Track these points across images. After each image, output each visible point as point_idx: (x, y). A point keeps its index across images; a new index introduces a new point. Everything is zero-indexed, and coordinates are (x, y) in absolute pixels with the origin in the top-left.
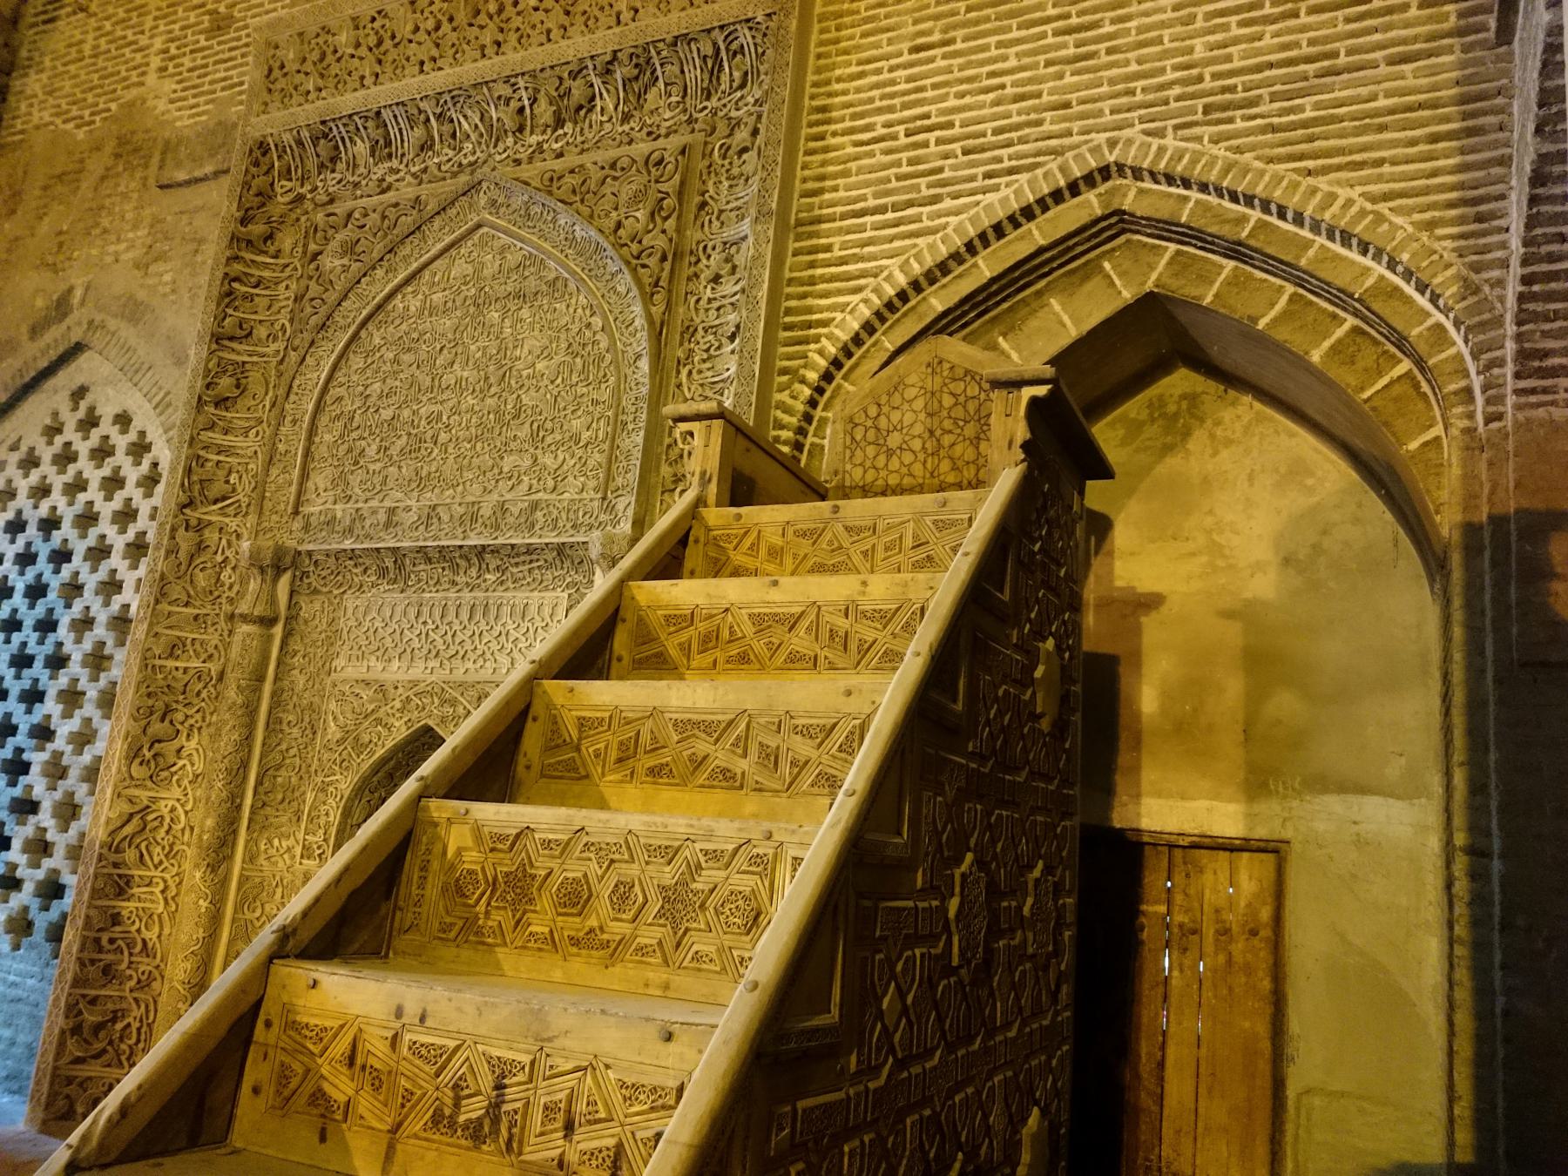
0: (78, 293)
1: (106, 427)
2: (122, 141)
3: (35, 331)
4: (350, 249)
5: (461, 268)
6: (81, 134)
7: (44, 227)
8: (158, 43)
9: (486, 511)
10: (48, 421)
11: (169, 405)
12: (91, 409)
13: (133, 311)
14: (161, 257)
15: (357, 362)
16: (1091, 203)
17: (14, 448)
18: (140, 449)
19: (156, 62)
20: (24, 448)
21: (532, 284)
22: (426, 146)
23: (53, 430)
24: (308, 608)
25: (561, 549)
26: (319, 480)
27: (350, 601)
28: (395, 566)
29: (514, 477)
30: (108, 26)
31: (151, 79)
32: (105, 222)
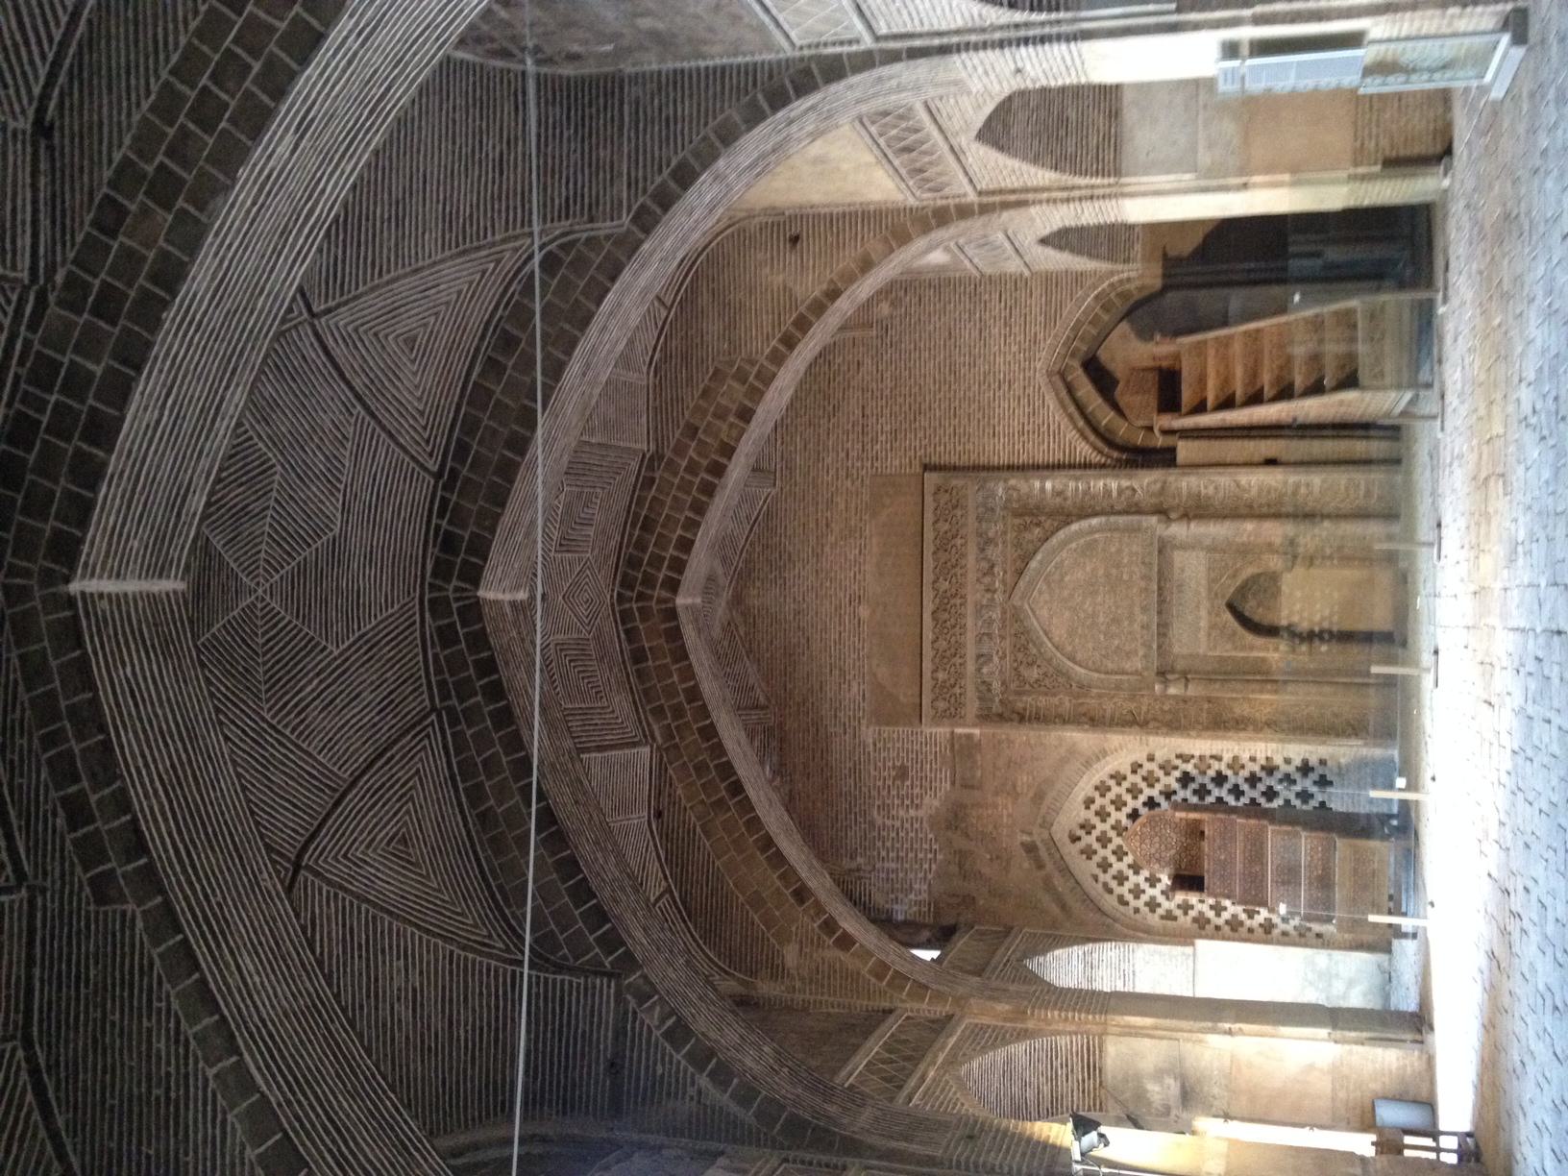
0: (1026, 838)
1: (1090, 815)
2: (948, 828)
3: (1041, 866)
4: (1030, 665)
5: (1045, 613)
6: (940, 857)
7: (986, 870)
8: (902, 813)
9: (1143, 584)
12: (1082, 827)
13: (1039, 797)
14: (1014, 787)
15: (1079, 656)
16: (1056, 378)
17: (1096, 878)
18: (1102, 789)
19: (912, 812)
20: (1098, 871)
21: (1056, 577)
22: (989, 635)
23: (1089, 853)
24: (1179, 667)
25: (1160, 552)
26: (1128, 666)
27: (1176, 650)
28: (1163, 628)
29: (1131, 573)
30: (883, 853)
31: (921, 813)
32: (991, 827)
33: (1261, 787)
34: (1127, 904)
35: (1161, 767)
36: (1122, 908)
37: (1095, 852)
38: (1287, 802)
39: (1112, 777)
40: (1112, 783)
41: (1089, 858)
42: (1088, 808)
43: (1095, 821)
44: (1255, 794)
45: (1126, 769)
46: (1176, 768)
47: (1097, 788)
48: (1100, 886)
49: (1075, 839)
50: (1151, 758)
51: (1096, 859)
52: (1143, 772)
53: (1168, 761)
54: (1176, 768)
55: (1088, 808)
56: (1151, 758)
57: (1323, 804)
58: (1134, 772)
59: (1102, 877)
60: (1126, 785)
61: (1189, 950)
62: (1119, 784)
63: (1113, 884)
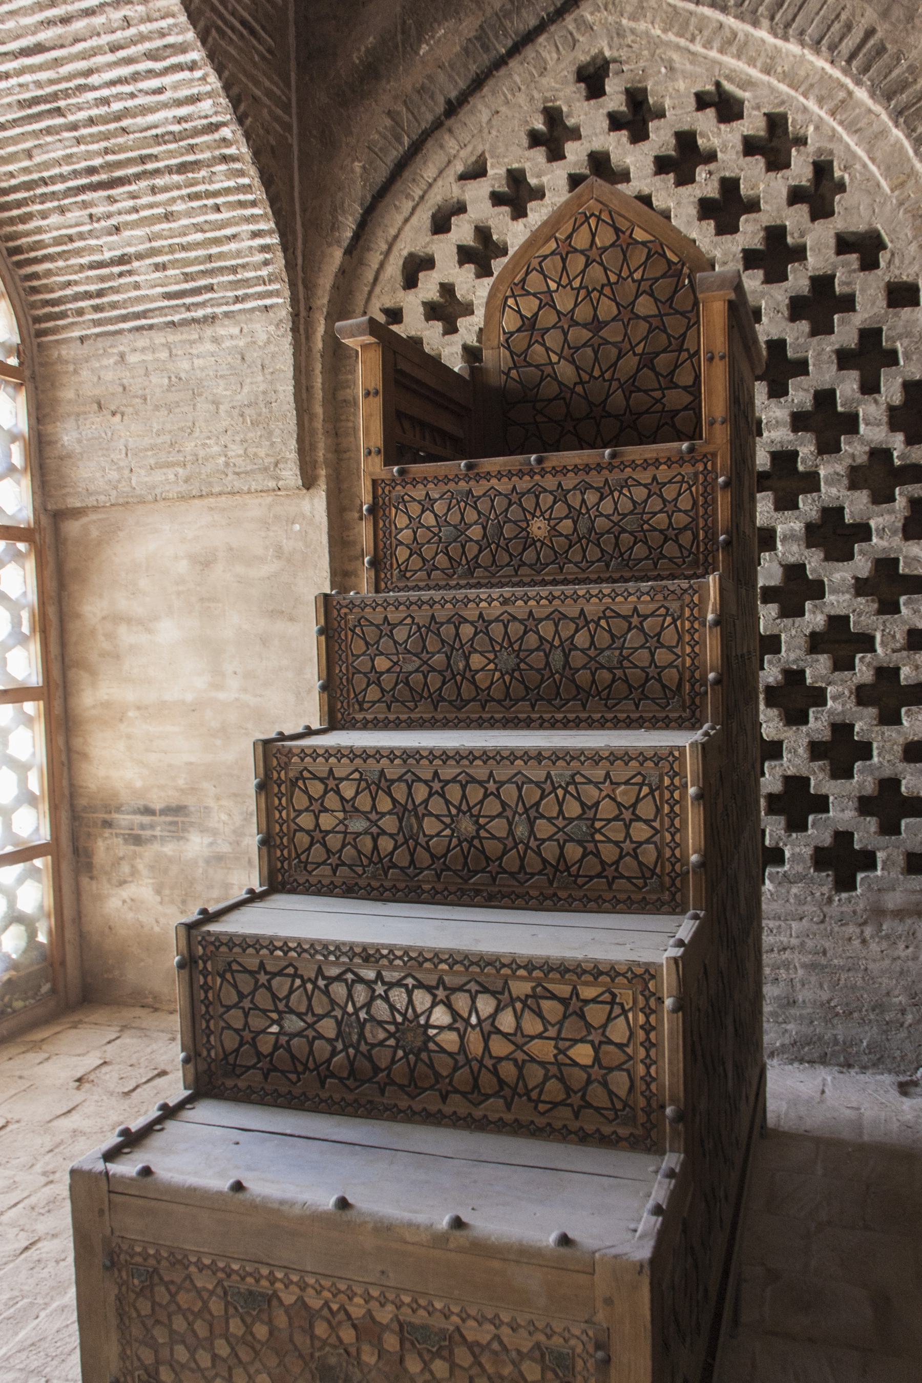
10: (539, 125)
11: (881, 50)
17: (477, 172)
20: (496, 172)
33: (817, 669)
34: (410, 282)
35: (870, 336)
36: (394, 269)
37: (556, 155)
38: (774, 750)
39: (822, 169)
40: (800, 170)
41: (535, 139)
42: (702, 101)
43: (661, 138)
44: (792, 651)
45: (852, 213)
46: (870, 387)
47: (776, 122)
48: (447, 189)
49: (592, 79)
50: (902, 295)
51: (533, 163)
52: (846, 274)
53: (891, 358)
54: (870, 387)
55: (702, 101)
56: (902, 295)
57: (776, 856)
58: (844, 244)
59: (477, 194)
60: (795, 219)
61: (291, 474)
62: (796, 196)
63: (462, 232)
